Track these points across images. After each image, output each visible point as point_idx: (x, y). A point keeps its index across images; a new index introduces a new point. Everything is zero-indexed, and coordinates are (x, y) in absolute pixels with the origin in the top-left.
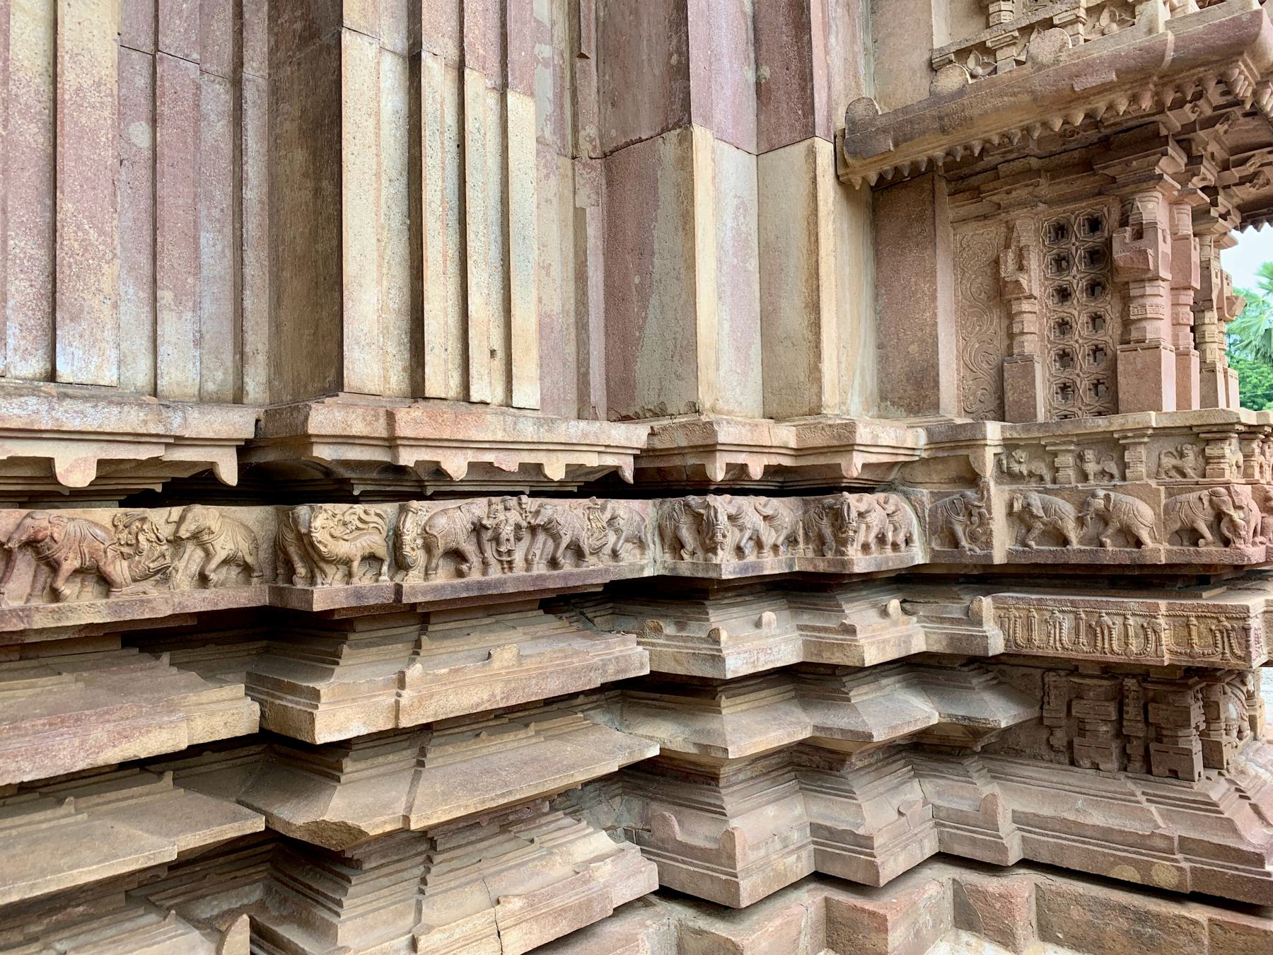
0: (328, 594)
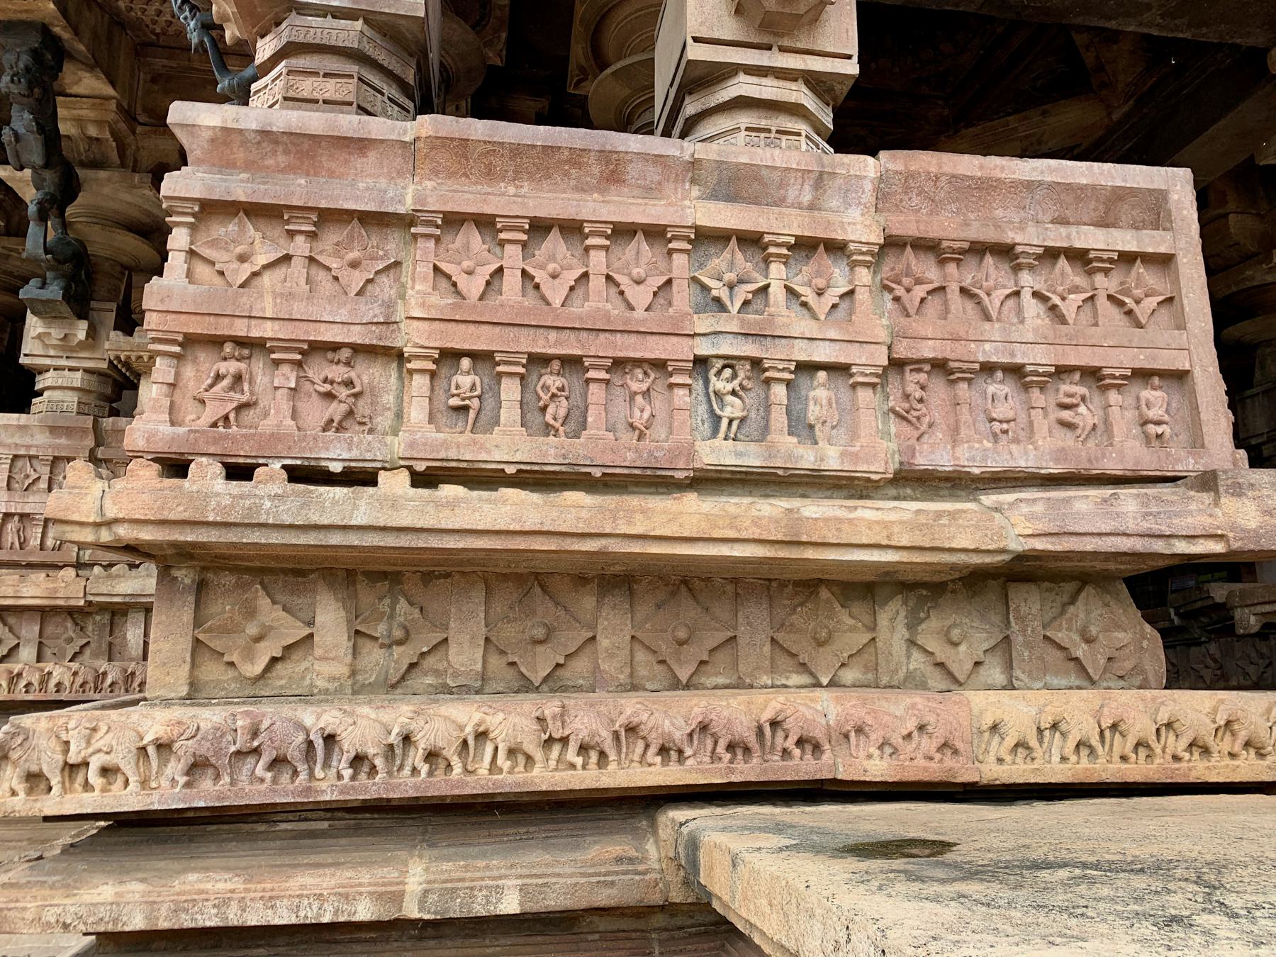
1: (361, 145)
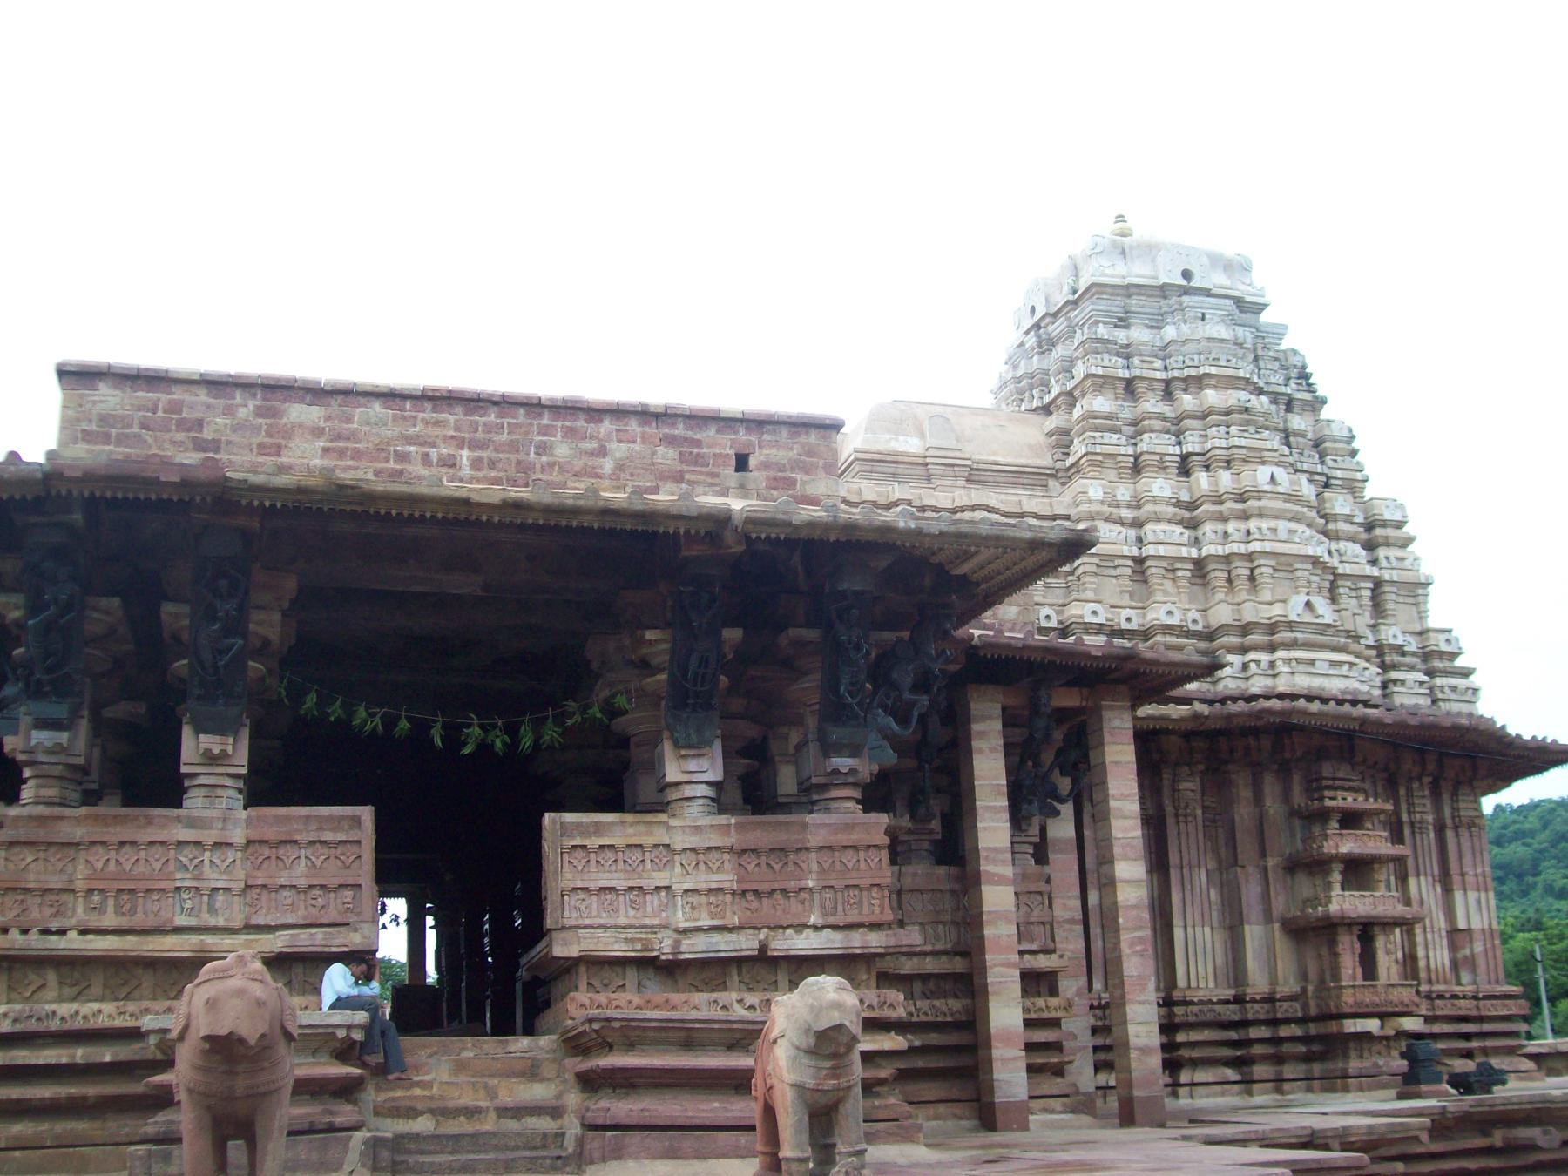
0: (1177, 1020)
1: (61, 818)
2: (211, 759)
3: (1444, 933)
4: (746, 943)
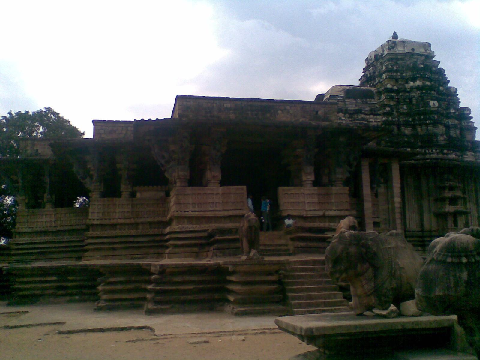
2: (214, 177)
3: (477, 217)
4: (320, 213)
